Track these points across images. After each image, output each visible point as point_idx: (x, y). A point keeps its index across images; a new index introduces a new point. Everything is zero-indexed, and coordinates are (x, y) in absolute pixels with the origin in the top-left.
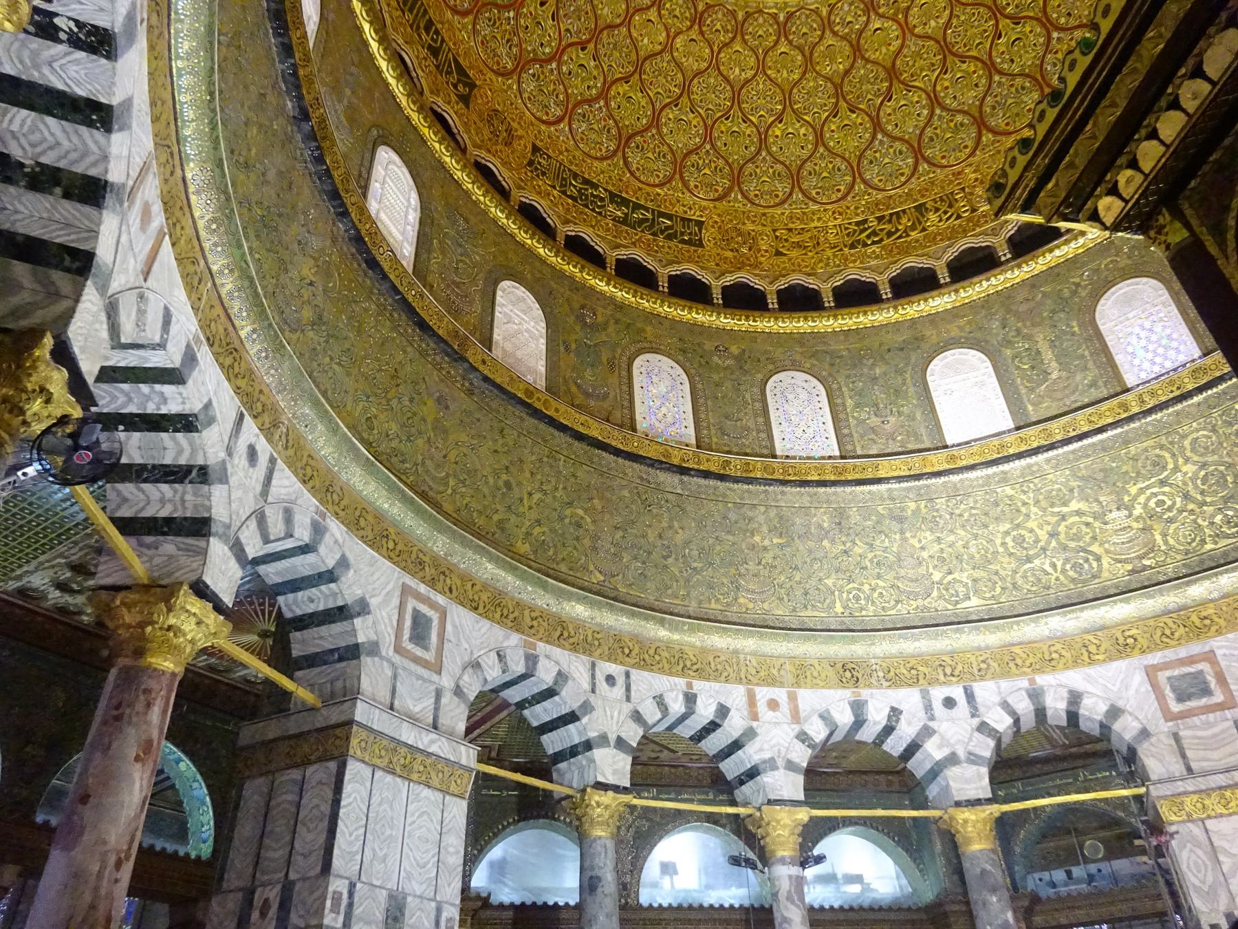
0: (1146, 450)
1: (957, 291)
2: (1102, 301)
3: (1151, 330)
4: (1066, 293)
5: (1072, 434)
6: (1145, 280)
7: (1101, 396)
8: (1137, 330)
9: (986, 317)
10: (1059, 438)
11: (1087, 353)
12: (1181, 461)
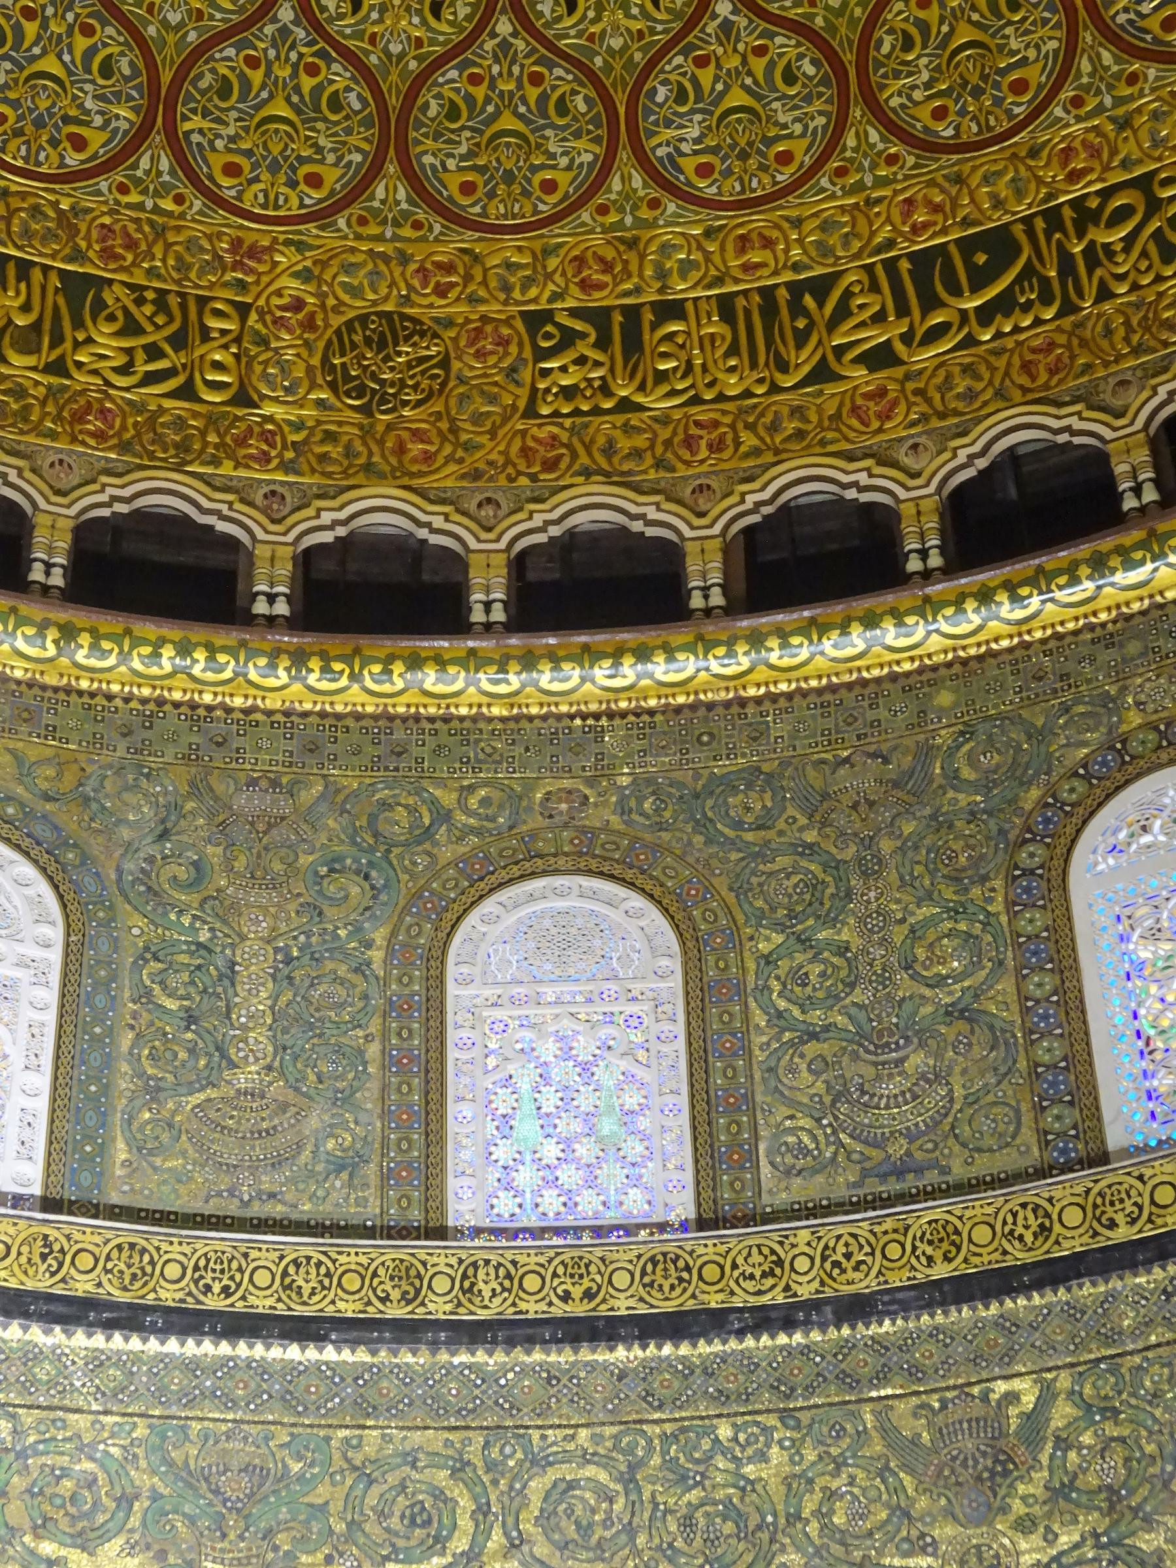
0: (411, 1459)
1: (68, 633)
2: (489, 906)
3: (586, 1069)
4: (398, 823)
5: (213, 1302)
6: (637, 902)
7: (352, 1212)
8: (548, 1050)
9: (120, 770)
10: (169, 1296)
11: (373, 1050)
12: (497, 1539)
